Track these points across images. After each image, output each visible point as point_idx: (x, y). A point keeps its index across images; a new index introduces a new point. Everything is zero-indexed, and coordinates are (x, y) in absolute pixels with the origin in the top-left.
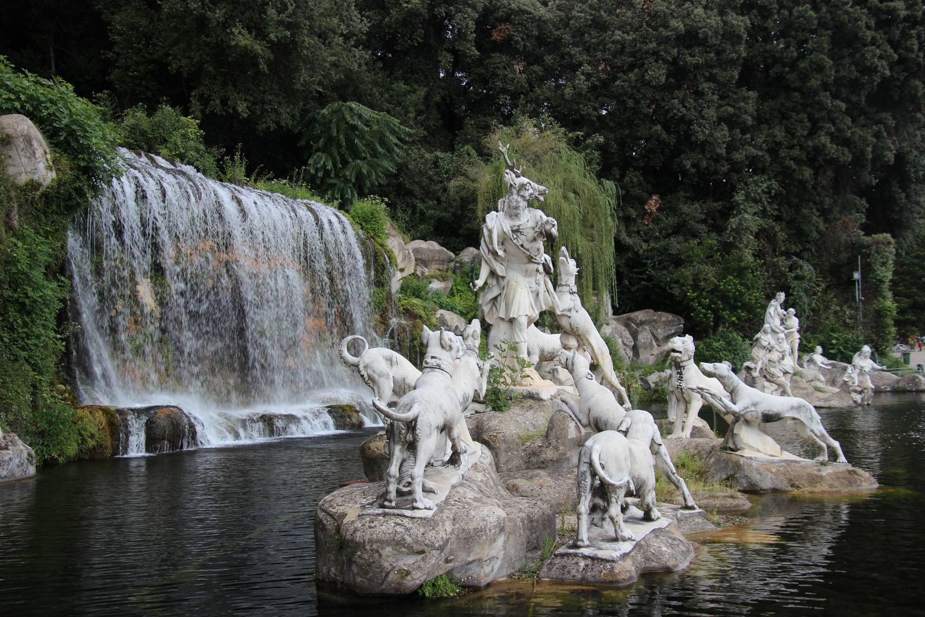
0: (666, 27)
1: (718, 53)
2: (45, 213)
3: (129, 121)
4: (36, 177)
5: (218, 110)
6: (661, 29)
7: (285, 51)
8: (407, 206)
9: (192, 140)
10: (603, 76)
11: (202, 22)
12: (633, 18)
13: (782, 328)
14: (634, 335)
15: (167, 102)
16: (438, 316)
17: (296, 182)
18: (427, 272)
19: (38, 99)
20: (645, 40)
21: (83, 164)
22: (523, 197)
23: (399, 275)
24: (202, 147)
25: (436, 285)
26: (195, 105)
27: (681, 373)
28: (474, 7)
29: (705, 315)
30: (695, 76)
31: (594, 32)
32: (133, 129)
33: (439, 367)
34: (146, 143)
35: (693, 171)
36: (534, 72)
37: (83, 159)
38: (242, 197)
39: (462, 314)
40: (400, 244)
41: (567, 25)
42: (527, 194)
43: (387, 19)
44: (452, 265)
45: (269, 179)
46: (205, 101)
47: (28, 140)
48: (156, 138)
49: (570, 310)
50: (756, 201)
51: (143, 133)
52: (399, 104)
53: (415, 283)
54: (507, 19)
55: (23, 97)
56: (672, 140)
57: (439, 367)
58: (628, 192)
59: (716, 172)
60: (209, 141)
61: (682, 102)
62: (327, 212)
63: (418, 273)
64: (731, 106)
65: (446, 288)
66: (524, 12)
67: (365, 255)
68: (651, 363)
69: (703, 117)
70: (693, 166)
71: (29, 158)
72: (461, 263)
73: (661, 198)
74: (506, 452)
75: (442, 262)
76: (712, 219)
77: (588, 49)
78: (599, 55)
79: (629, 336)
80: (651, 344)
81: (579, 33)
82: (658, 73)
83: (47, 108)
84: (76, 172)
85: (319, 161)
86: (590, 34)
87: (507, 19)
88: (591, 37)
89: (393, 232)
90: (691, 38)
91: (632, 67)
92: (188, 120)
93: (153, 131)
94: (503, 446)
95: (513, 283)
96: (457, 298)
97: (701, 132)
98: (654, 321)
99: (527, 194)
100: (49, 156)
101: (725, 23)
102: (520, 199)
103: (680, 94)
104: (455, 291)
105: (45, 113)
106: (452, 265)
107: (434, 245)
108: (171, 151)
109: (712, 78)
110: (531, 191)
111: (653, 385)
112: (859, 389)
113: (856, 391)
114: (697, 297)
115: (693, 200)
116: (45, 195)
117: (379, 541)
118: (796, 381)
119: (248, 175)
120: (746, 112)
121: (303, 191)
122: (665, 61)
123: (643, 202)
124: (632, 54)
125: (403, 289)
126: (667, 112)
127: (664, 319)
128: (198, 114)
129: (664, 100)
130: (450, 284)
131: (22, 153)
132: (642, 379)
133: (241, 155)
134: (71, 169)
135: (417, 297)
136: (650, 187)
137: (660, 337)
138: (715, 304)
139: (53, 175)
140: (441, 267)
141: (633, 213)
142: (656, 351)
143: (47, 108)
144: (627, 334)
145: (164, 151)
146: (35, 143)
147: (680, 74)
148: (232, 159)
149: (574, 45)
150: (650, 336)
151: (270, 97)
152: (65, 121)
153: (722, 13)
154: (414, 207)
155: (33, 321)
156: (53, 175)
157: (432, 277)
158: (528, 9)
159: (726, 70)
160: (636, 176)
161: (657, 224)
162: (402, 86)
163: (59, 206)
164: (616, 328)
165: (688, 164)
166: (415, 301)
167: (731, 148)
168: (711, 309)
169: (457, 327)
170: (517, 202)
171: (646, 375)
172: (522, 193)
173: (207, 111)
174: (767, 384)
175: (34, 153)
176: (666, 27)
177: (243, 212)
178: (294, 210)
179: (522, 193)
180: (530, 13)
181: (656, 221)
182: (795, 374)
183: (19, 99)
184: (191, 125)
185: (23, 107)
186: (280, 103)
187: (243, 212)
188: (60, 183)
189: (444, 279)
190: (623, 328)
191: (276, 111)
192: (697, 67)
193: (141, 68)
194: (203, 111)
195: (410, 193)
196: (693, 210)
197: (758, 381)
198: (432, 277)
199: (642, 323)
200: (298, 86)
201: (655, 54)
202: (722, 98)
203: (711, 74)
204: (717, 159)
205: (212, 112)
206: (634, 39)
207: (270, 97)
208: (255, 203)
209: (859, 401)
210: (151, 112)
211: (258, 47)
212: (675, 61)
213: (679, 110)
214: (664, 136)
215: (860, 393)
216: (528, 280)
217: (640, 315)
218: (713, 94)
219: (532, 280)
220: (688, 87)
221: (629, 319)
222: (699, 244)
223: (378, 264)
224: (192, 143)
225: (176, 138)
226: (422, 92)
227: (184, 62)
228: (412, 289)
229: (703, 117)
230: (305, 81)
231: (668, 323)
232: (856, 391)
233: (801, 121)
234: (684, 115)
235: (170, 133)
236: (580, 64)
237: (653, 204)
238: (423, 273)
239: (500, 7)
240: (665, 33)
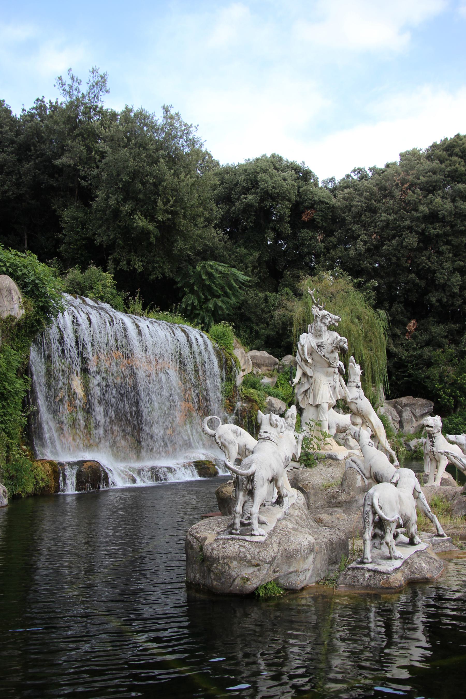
0: (416, 210)
1: (452, 226)
2: (17, 336)
3: (70, 276)
4: (13, 314)
5: (125, 268)
6: (413, 212)
7: (168, 230)
8: (247, 328)
9: (109, 287)
10: (375, 243)
11: (116, 213)
12: (394, 205)
14: (400, 414)
15: (93, 264)
16: (267, 401)
17: (175, 313)
18: (260, 371)
19: (16, 265)
20: (402, 218)
21: (41, 304)
22: (324, 323)
24: (115, 291)
25: (266, 380)
26: (111, 265)
27: (433, 442)
28: (289, 200)
29: (448, 400)
30: (437, 242)
31: (368, 214)
32: (72, 281)
33: (269, 439)
34: (80, 290)
35: (437, 304)
37: (42, 301)
38: (140, 324)
39: (283, 399)
40: (242, 353)
41: (350, 210)
42: (327, 322)
43: (233, 208)
44: (277, 366)
45: (157, 311)
46: (117, 262)
47: (9, 290)
48: (86, 287)
49: (357, 399)
51: (78, 284)
52: (242, 261)
53: (252, 379)
54: (312, 207)
55: (8, 264)
56: (423, 284)
57: (269, 439)
58: (394, 318)
59: (453, 305)
60: (119, 287)
61: (428, 258)
62: (195, 332)
63: (255, 372)
64: (462, 261)
65: (273, 382)
66: (322, 202)
67: (220, 361)
68: (412, 432)
69: (443, 268)
70: (438, 301)
71: (10, 301)
72: (283, 366)
73: (417, 322)
74: (314, 495)
75: (270, 365)
76: (451, 335)
77: (365, 226)
79: (396, 414)
80: (411, 419)
81: (359, 215)
82: (412, 240)
83: (21, 270)
84: (36, 310)
85: (190, 299)
86: (365, 215)
87: (312, 207)
89: (238, 345)
90: (433, 217)
91: (394, 237)
92: (107, 274)
93: (84, 282)
94: (312, 492)
95: (318, 381)
96: (280, 389)
97: (441, 278)
98: (413, 404)
99: (327, 322)
100: (21, 300)
101: (456, 207)
102: (322, 325)
103: (427, 253)
104: (279, 384)
105: (20, 273)
106: (277, 366)
107: (264, 354)
108: (95, 294)
109: (448, 243)
110: (330, 320)
111: (413, 448)
114: (443, 388)
115: (438, 323)
116: (18, 324)
117: (228, 557)
119: (144, 309)
121: (178, 318)
122: (417, 233)
123: (405, 325)
125: (244, 383)
126: (419, 265)
127: (420, 403)
128: (112, 270)
129: (416, 257)
130: (275, 379)
131: (5, 299)
132: (406, 444)
133: (139, 296)
134: (34, 308)
135: (254, 388)
136: (409, 314)
137: (418, 415)
138: (454, 393)
139: (23, 312)
140: (269, 368)
141: (398, 332)
142: (415, 424)
143: (21, 270)
144: (395, 413)
145: (91, 295)
146: (13, 292)
147: (426, 240)
148: (134, 299)
150: (410, 414)
151: (158, 259)
152: (32, 278)
153: (453, 201)
154: (251, 328)
155: (8, 405)
156: (23, 312)
157: (264, 375)
158: (326, 200)
159: (457, 237)
160: (400, 307)
161: (415, 339)
162: (243, 250)
163: (26, 331)
164: (388, 409)
165: (434, 300)
166: (252, 391)
168: (452, 396)
169: (280, 408)
170: (320, 327)
171: (409, 440)
172: (323, 321)
173: (118, 269)
175: (12, 298)
176: (416, 210)
177: (140, 333)
178: (173, 332)
179: (323, 321)
180: (327, 204)
181: (414, 337)
183: (5, 265)
184: (108, 278)
185: (7, 270)
186: (164, 263)
187: (140, 333)
188: (27, 317)
189: (271, 376)
190: (393, 409)
191: (161, 267)
192: (438, 236)
193: (79, 243)
194: (115, 269)
195: (249, 319)
196: (438, 330)
198: (264, 375)
199: (405, 405)
200: (176, 252)
201: (409, 228)
202: (455, 255)
203: (447, 240)
204: (453, 295)
205: (121, 269)
206: (395, 219)
207: (158, 259)
208: (148, 327)
210: (83, 270)
212: (422, 233)
213: (426, 264)
214: (417, 280)
216: (328, 378)
217: (404, 400)
218: (450, 253)
219: (331, 379)
220: (432, 249)
221: (396, 403)
222: (443, 352)
223: (228, 366)
224: (108, 289)
225: (99, 286)
226: (256, 254)
227: (105, 238)
228: (252, 383)
229: (443, 268)
230: (180, 248)
231: (422, 406)
234: (430, 267)
235: (95, 283)
237: (412, 325)
238: (257, 372)
239: (306, 200)
240: (416, 214)
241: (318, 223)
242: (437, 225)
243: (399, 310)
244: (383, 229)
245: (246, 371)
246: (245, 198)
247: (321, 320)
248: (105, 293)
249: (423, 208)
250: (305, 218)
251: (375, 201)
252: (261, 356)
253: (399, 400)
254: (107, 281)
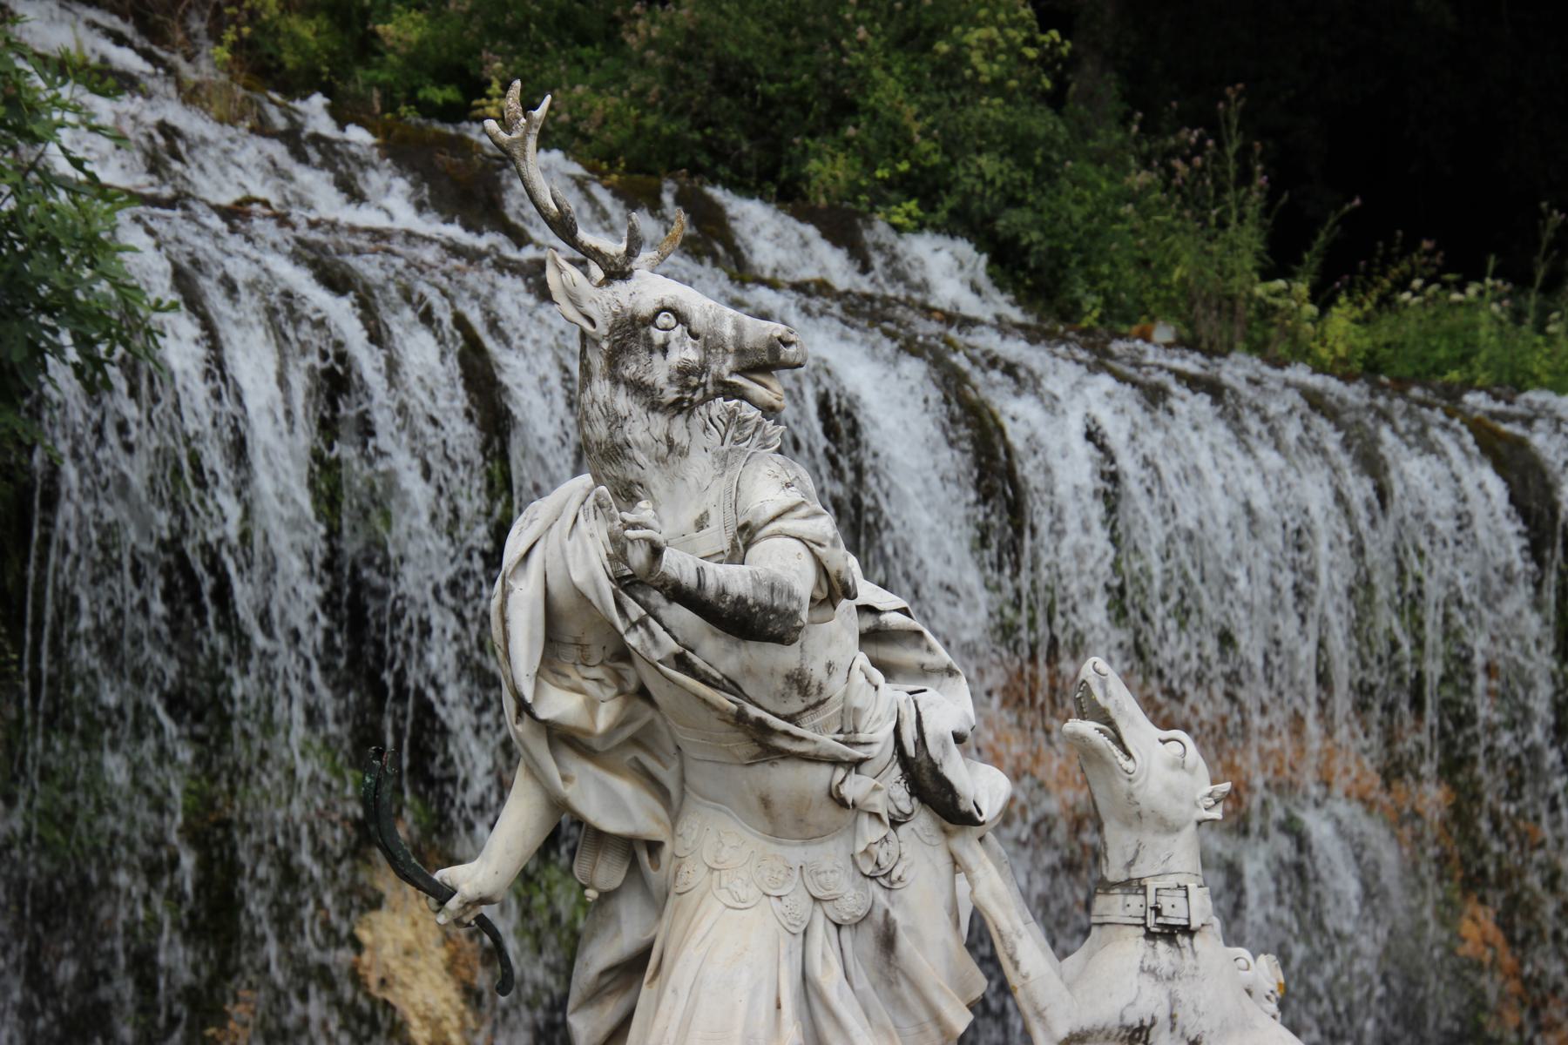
22: (639, 388)
42: (659, 372)
95: (694, 875)
102: (623, 402)
108: (870, 165)
110: (685, 353)
119: (1279, 262)
170: (616, 420)
172: (630, 370)
178: (1372, 464)
179: (630, 370)
216: (796, 853)
219: (829, 859)
224: (991, 109)
247: (614, 359)
248: (952, 145)
254: (975, 36)
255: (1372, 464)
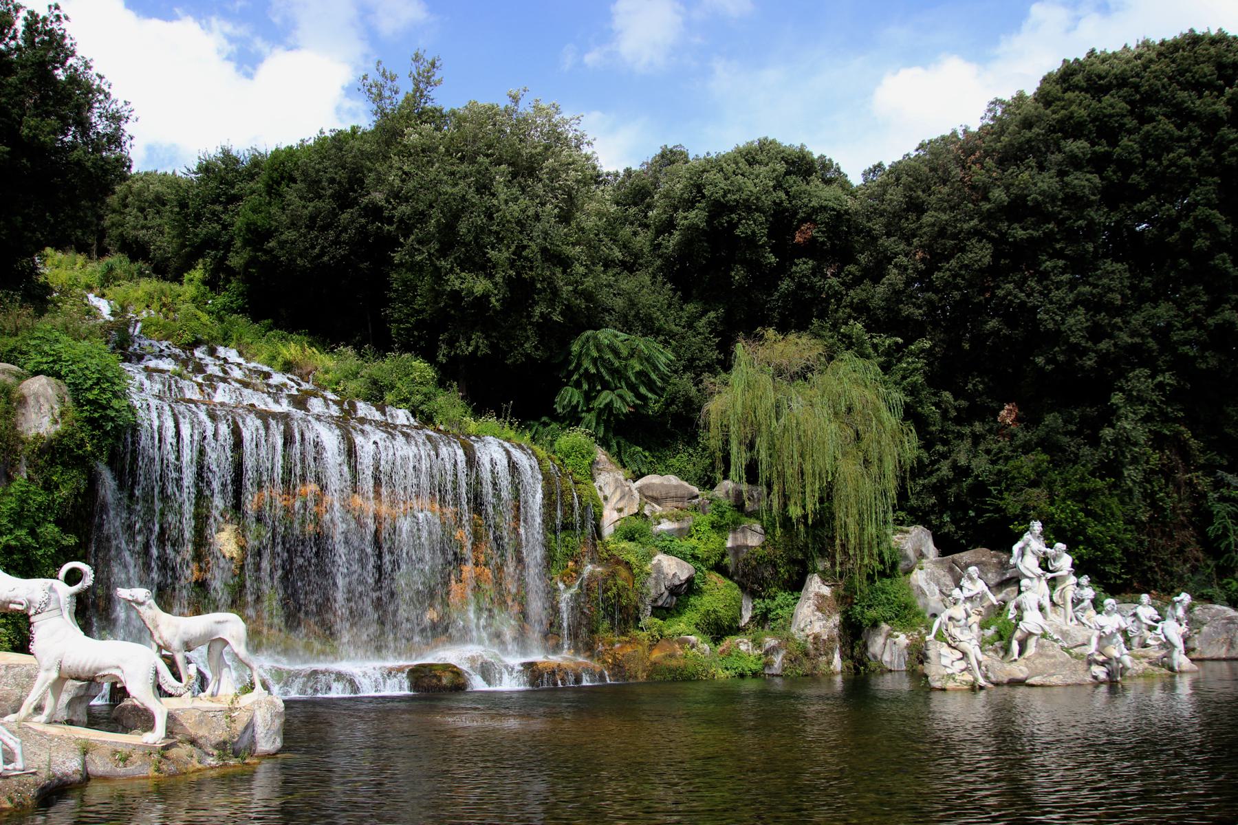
1: (1060, 223)
10: (921, 266)
13: (1040, 571)
23: (616, 515)
31: (912, 216)
36: (850, 273)
40: (617, 480)
50: (1141, 400)
54: (808, 219)
56: (1019, 333)
67: (548, 495)
78: (916, 241)
86: (907, 219)
87: (808, 219)
88: (908, 225)
89: (608, 466)
90: (1018, 209)
107: (673, 480)
109: (1059, 254)
112: (1101, 658)
113: (1097, 662)
118: (1042, 646)
120: (1111, 290)
122: (990, 239)
124: (954, 236)
135: (632, 539)
140: (680, 505)
146: (42, 400)
149: (889, 235)
153: (1061, 174)
157: (661, 517)
164: (932, 573)
167: (1096, 333)
169: (674, 575)
174: (945, 650)
180: (834, 209)
182: (1044, 636)
197: (931, 646)
198: (661, 517)
201: (976, 232)
209: (1103, 676)
211: (480, 285)
213: (1016, 297)
215: (1102, 664)
217: (966, 556)
232: (1097, 662)
233: (1194, 294)
234: (1023, 303)
236: (896, 254)
237: (1007, 414)
238: (653, 512)
241: (823, 243)
242: (1030, 220)
243: (980, 387)
244: (934, 239)
245: (626, 510)
246: (686, 218)
249: (998, 194)
250: (799, 238)
251: (924, 191)
252: (662, 485)
253: (956, 556)
255: (436, 449)
